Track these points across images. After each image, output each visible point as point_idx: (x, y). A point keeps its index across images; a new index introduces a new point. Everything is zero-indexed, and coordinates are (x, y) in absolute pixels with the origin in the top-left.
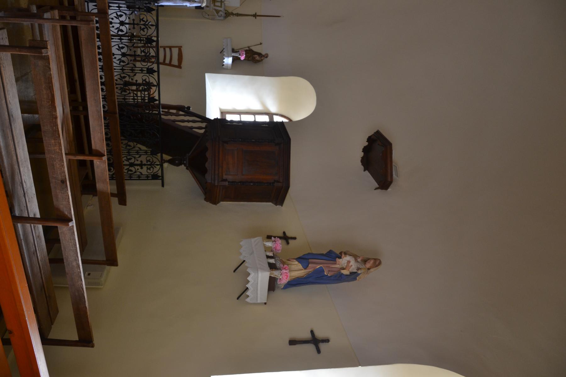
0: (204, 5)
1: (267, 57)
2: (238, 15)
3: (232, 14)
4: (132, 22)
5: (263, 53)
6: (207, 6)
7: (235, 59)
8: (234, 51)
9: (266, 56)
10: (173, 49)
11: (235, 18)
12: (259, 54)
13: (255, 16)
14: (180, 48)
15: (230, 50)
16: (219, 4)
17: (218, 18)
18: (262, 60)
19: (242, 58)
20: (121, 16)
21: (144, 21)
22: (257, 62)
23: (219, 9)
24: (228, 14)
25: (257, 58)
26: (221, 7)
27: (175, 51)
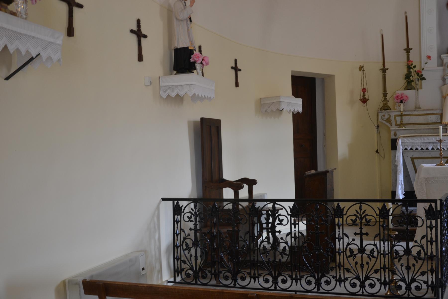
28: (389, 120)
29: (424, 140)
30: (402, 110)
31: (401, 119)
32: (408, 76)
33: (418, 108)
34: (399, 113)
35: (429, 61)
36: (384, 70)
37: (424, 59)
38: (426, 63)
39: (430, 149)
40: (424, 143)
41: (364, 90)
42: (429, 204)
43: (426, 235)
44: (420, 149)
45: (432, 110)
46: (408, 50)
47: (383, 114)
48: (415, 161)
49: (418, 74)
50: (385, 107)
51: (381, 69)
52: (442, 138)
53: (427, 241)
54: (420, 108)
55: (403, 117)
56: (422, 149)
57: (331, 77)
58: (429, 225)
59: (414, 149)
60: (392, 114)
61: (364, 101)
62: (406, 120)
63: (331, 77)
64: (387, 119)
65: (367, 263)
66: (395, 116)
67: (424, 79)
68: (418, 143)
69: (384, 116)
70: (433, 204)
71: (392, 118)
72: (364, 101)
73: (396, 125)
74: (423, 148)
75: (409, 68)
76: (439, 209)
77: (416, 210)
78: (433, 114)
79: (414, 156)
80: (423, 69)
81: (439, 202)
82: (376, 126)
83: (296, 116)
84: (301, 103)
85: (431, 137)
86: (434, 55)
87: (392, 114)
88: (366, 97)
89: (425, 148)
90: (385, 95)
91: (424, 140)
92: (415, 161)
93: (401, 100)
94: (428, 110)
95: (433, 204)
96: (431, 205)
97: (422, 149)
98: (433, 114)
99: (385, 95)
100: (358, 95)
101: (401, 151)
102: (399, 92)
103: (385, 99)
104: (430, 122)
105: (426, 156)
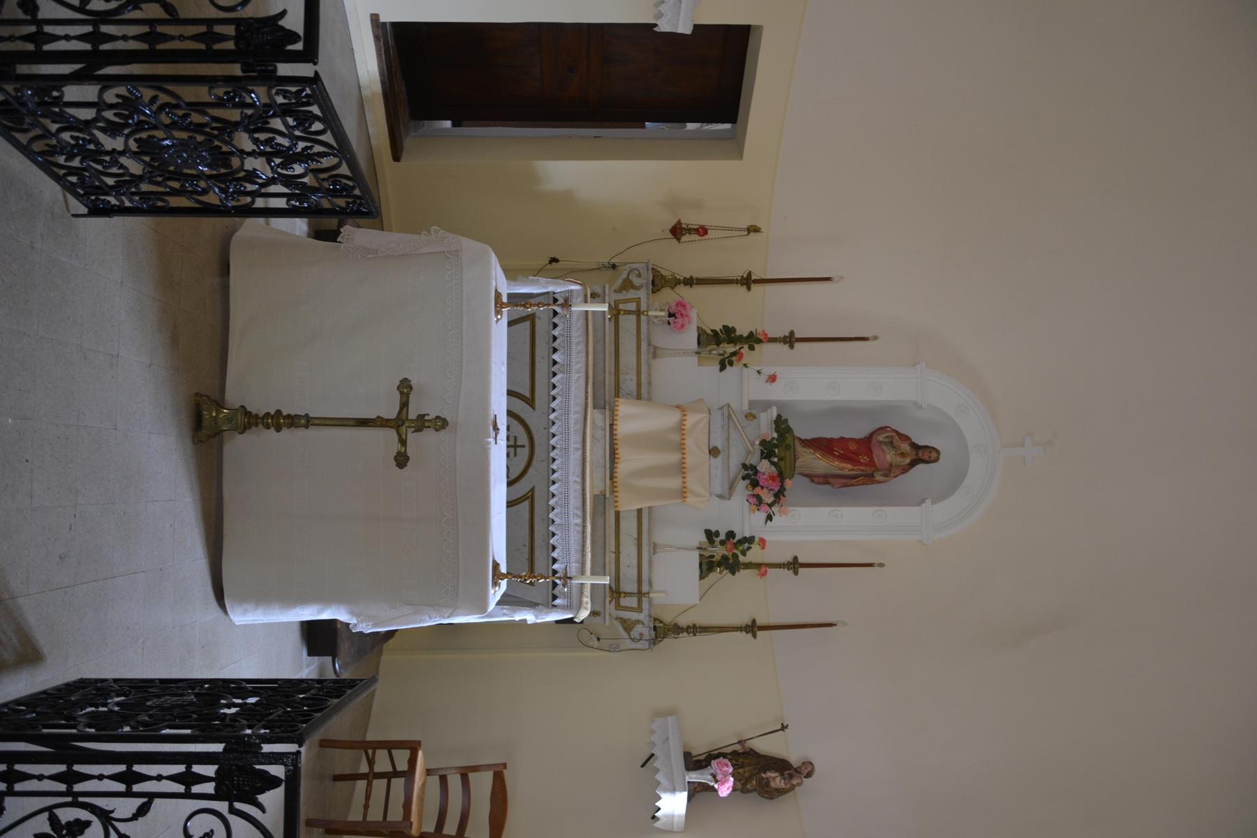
0: (584, 614)
1: (809, 775)
2: (694, 630)
3: (677, 630)
5: (794, 758)
6: (594, 613)
7: (696, 791)
8: (694, 762)
9: (807, 770)
10: (471, 776)
11: (685, 639)
12: (781, 766)
13: (752, 628)
14: (499, 780)
15: (679, 762)
16: (632, 602)
17: (628, 644)
18: (793, 788)
19: (725, 790)
22: (769, 793)
23: (634, 616)
24: (663, 631)
25: (777, 781)
26: (639, 609)
27: (482, 784)
28: (627, 285)
29: (578, 344)
30: (651, 313)
31: (629, 312)
32: (729, 334)
33: (655, 353)
34: (643, 307)
35: (764, 377)
36: (747, 281)
37: (768, 371)
38: (759, 372)
39: (555, 357)
40: (569, 342)
41: (702, 231)
42: (300, 30)
43: (175, 20)
44: (556, 333)
45: (650, 383)
46: (790, 340)
47: (644, 273)
48: (527, 324)
49: (733, 354)
50: (659, 282)
51: (750, 274)
52: (578, 308)
53: (151, 22)
54: (655, 356)
55: (633, 317)
56: (555, 338)
57: (760, 28)
58: (218, 29)
59: (555, 320)
60: (642, 294)
61: (677, 231)
62: (628, 322)
63: (738, 153)
64: (631, 282)
66: (638, 301)
67: (723, 368)
68: (569, 328)
69: (639, 276)
70: (299, 46)
71: (632, 294)
72: (677, 231)
73: (617, 303)
74: (558, 341)
75: (753, 340)
76: (284, 69)
77: (317, 78)
78: (639, 385)
79: (537, 320)
80: (745, 365)
81: (304, 70)
82: (613, 261)
83: (650, 27)
84: (679, 31)
85: (584, 359)
86: (776, 393)
87: (642, 294)
88: (685, 238)
89: (556, 345)
90: (689, 282)
91: (578, 344)
92: (527, 324)
93: (675, 315)
94: (650, 375)
95: (299, 46)
96: (292, 36)
97: (555, 338)
98: (639, 385)
99: (689, 282)
100: (691, 219)
101: (550, 289)
102: (693, 314)
103: (678, 282)
104: (621, 377)
105: (538, 350)
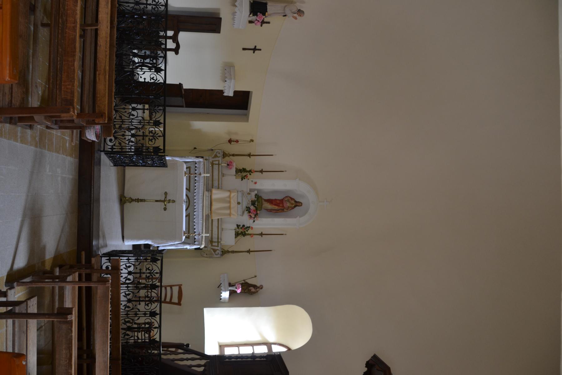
0: (203, 246)
1: (261, 288)
2: (233, 252)
3: (228, 252)
4: (139, 271)
5: (258, 285)
6: (205, 247)
7: (232, 293)
8: (230, 285)
9: (261, 287)
10: (173, 288)
11: (231, 254)
12: (255, 286)
13: (249, 251)
14: (180, 287)
15: (227, 285)
16: (216, 244)
17: (215, 256)
18: (257, 291)
19: (239, 291)
20: (130, 267)
21: (149, 270)
22: (252, 293)
23: (216, 248)
24: (224, 252)
25: (253, 290)
26: (218, 246)
27: (176, 290)
28: (216, 156)
32: (244, 170)
33: (223, 175)
34: (220, 163)
36: (249, 155)
37: (255, 181)
41: (237, 141)
46: (262, 171)
50: (225, 155)
52: (203, 175)
54: (223, 176)
61: (230, 141)
62: (216, 167)
63: (247, 120)
65: (126, 112)
66: (219, 161)
67: (242, 180)
71: (217, 159)
72: (230, 141)
73: (213, 161)
75: (250, 171)
76: (160, 154)
78: (219, 184)
83: (222, 92)
86: (257, 187)
87: (220, 159)
88: (232, 143)
90: (233, 155)
93: (229, 165)
95: (162, 151)
98: (219, 184)
99: (233, 155)
100: (234, 138)
102: (234, 164)
103: (230, 155)
